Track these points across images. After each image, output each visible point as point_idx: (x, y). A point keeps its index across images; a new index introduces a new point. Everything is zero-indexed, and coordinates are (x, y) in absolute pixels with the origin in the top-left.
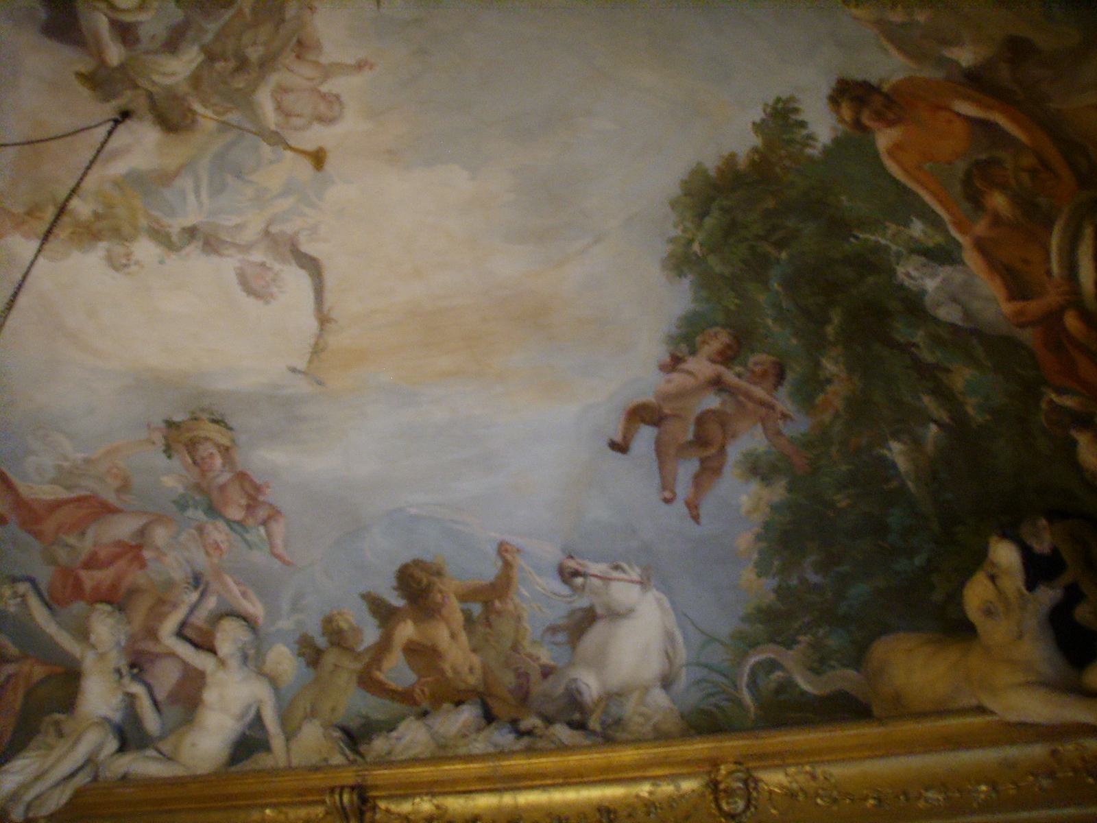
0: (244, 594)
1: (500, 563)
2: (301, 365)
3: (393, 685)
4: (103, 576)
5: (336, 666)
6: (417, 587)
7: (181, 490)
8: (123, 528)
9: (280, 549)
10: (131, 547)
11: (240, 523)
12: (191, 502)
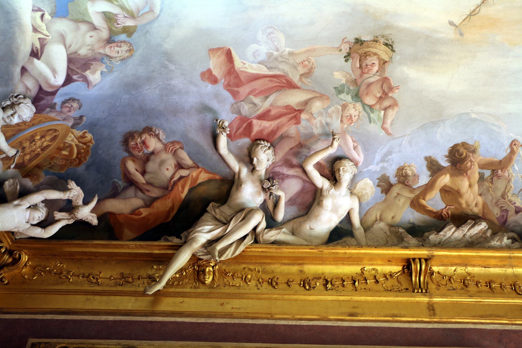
0: (355, 148)
1: (509, 151)
2: (457, 22)
3: (430, 208)
4: (268, 125)
5: (398, 194)
6: (458, 158)
7: (344, 81)
8: (293, 99)
9: (388, 125)
10: (295, 110)
11: (371, 107)
12: (346, 90)
